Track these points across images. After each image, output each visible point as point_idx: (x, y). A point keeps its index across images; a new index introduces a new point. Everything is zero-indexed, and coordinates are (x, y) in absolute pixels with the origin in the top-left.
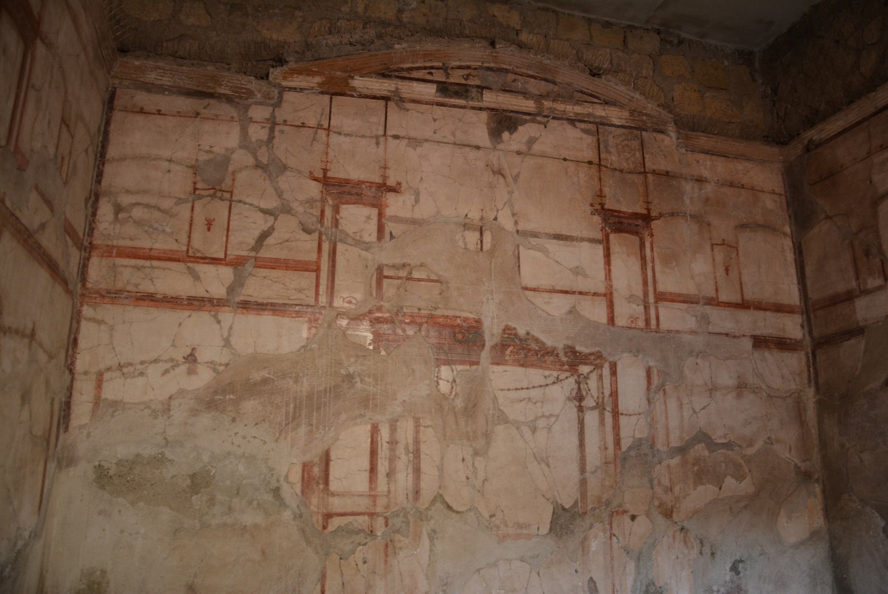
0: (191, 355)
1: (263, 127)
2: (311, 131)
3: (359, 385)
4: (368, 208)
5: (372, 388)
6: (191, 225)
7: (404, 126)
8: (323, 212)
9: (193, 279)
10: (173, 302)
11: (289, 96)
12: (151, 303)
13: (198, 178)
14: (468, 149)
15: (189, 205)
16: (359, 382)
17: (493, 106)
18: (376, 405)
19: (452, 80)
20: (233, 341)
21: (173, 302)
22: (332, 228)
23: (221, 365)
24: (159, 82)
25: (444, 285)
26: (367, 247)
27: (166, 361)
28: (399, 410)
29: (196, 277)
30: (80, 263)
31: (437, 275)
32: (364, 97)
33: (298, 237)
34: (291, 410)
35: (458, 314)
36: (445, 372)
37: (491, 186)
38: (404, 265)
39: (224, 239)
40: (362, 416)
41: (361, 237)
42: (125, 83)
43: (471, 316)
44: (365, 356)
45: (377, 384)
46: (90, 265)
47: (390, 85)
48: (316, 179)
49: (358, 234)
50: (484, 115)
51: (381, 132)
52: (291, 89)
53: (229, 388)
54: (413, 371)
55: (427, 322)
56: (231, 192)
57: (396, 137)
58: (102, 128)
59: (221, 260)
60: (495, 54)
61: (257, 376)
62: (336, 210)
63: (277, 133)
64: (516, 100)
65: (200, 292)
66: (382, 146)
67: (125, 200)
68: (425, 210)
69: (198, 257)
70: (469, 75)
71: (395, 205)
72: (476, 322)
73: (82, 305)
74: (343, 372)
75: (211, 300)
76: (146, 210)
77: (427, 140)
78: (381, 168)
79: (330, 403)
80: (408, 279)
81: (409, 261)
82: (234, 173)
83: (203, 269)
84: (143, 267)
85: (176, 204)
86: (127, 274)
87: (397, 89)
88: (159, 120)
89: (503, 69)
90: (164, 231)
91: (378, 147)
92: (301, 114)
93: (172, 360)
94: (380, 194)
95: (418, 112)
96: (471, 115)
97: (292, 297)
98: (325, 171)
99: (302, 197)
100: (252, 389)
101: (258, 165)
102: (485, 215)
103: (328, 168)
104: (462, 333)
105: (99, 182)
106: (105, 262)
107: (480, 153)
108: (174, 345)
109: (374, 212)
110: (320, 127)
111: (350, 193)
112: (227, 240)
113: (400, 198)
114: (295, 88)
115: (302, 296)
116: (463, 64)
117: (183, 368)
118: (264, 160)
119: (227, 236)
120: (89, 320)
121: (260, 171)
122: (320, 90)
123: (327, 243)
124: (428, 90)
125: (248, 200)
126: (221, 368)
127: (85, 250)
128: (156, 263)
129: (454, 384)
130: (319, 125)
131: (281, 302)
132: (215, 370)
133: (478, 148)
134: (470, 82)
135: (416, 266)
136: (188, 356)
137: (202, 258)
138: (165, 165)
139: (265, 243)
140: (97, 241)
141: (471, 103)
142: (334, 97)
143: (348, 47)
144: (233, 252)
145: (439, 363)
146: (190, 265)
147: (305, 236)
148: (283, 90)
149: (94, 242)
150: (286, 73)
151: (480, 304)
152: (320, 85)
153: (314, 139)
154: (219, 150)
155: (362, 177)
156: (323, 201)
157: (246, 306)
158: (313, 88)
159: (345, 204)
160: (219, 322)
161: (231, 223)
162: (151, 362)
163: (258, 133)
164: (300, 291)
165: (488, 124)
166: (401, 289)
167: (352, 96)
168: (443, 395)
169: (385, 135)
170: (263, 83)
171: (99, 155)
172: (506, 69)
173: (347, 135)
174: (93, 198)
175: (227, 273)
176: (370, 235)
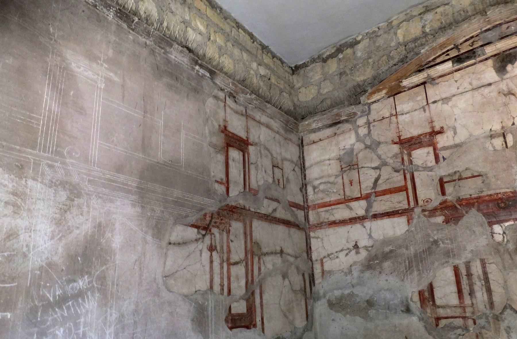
0: (356, 245)
1: (365, 128)
2: (388, 120)
3: (442, 245)
4: (427, 148)
5: (450, 246)
6: (344, 185)
7: (438, 94)
8: (403, 159)
9: (349, 210)
10: (343, 222)
11: (373, 107)
12: (335, 225)
13: (342, 163)
14: (483, 89)
15: (341, 177)
16: (442, 244)
17: (495, 53)
18: (455, 255)
19: (462, 51)
20: (373, 235)
21: (343, 222)
22: (409, 165)
23: (370, 247)
24: (317, 127)
25: (484, 177)
26: (431, 169)
27: (346, 250)
28: (470, 256)
29: (351, 209)
30: (305, 215)
31: (478, 172)
32: (411, 89)
33: (393, 176)
34: (407, 264)
35: (498, 191)
36: (497, 229)
37: (506, 105)
38: (455, 173)
39: (359, 187)
40: (447, 262)
41: (426, 165)
42: (305, 133)
43: (508, 190)
44: (442, 229)
45: (453, 243)
46: (309, 215)
47: (423, 75)
48: (395, 143)
49: (424, 164)
50: (490, 62)
51: (426, 103)
52: (373, 103)
53: (376, 257)
54: (473, 231)
55: (477, 202)
56: (357, 165)
57: (435, 102)
58: (301, 156)
59: (360, 198)
60: (487, 20)
61: (387, 249)
62: (410, 155)
63: (371, 128)
64: (511, 41)
65: (354, 215)
66: (427, 111)
67: (316, 183)
68: (462, 137)
69: (350, 199)
70: (474, 42)
71: (442, 141)
72: (512, 193)
73: (310, 232)
74: (431, 240)
75: (359, 218)
76: (325, 185)
77: (454, 96)
78: (429, 123)
79: (427, 258)
80: (459, 180)
81: (458, 170)
82: (357, 155)
83: (353, 204)
84: (329, 210)
85: (336, 178)
86: (323, 215)
87: (428, 75)
88: (321, 143)
89: (497, 25)
90: (333, 192)
91: (425, 113)
92: (381, 113)
93: (348, 249)
94: (432, 138)
95: (445, 81)
96: (480, 67)
97: (397, 207)
98: (399, 137)
99: (390, 155)
100: (386, 256)
101: (367, 147)
102: (504, 124)
103: (400, 135)
104: (504, 202)
105: (305, 179)
106: (314, 212)
107: (493, 87)
108: (347, 242)
109: (431, 149)
110: (392, 115)
111: (415, 144)
112: (360, 187)
113: (445, 136)
114: (375, 101)
115: (401, 205)
116: (467, 37)
117: (353, 252)
118: (368, 143)
119: (360, 185)
120: (314, 238)
121: (368, 150)
122: (387, 96)
123: (409, 174)
124: (447, 66)
125: (366, 166)
126: (370, 249)
127: (306, 209)
128: (333, 207)
129: (504, 235)
130: (391, 115)
131: (391, 210)
132: (367, 250)
133: (490, 84)
134: (474, 46)
135: (463, 171)
136: (355, 245)
137: (351, 199)
138: (328, 162)
139: (378, 183)
140: (310, 204)
141: (478, 59)
142: (395, 96)
143: (394, 67)
144: (364, 192)
145: (491, 224)
146: (347, 204)
147: (397, 174)
148: (369, 105)
149: (309, 205)
150: (368, 96)
151: (513, 182)
152: (386, 94)
153: (390, 123)
154: (348, 147)
155: (420, 132)
156: (402, 153)
157: (375, 216)
158: (383, 97)
159: (413, 150)
160: (365, 227)
161: (360, 179)
162: (340, 252)
163: (363, 131)
164: (400, 202)
165: (494, 67)
166: (456, 187)
167: (405, 91)
168: (498, 242)
169: (428, 104)
170: (360, 106)
171: (303, 168)
172: (499, 24)
173: (406, 114)
174: (304, 187)
175: (363, 203)
176: (431, 162)
